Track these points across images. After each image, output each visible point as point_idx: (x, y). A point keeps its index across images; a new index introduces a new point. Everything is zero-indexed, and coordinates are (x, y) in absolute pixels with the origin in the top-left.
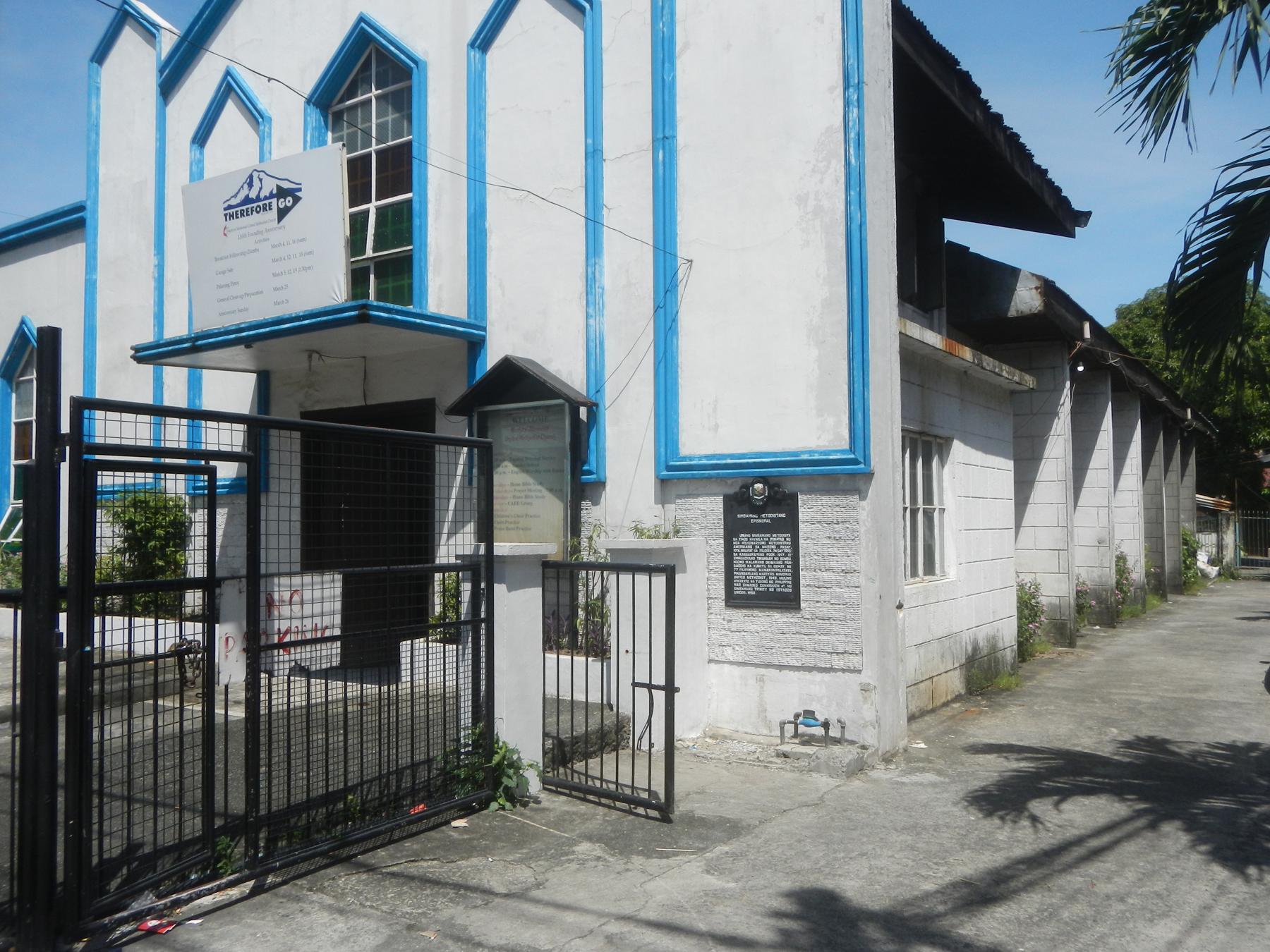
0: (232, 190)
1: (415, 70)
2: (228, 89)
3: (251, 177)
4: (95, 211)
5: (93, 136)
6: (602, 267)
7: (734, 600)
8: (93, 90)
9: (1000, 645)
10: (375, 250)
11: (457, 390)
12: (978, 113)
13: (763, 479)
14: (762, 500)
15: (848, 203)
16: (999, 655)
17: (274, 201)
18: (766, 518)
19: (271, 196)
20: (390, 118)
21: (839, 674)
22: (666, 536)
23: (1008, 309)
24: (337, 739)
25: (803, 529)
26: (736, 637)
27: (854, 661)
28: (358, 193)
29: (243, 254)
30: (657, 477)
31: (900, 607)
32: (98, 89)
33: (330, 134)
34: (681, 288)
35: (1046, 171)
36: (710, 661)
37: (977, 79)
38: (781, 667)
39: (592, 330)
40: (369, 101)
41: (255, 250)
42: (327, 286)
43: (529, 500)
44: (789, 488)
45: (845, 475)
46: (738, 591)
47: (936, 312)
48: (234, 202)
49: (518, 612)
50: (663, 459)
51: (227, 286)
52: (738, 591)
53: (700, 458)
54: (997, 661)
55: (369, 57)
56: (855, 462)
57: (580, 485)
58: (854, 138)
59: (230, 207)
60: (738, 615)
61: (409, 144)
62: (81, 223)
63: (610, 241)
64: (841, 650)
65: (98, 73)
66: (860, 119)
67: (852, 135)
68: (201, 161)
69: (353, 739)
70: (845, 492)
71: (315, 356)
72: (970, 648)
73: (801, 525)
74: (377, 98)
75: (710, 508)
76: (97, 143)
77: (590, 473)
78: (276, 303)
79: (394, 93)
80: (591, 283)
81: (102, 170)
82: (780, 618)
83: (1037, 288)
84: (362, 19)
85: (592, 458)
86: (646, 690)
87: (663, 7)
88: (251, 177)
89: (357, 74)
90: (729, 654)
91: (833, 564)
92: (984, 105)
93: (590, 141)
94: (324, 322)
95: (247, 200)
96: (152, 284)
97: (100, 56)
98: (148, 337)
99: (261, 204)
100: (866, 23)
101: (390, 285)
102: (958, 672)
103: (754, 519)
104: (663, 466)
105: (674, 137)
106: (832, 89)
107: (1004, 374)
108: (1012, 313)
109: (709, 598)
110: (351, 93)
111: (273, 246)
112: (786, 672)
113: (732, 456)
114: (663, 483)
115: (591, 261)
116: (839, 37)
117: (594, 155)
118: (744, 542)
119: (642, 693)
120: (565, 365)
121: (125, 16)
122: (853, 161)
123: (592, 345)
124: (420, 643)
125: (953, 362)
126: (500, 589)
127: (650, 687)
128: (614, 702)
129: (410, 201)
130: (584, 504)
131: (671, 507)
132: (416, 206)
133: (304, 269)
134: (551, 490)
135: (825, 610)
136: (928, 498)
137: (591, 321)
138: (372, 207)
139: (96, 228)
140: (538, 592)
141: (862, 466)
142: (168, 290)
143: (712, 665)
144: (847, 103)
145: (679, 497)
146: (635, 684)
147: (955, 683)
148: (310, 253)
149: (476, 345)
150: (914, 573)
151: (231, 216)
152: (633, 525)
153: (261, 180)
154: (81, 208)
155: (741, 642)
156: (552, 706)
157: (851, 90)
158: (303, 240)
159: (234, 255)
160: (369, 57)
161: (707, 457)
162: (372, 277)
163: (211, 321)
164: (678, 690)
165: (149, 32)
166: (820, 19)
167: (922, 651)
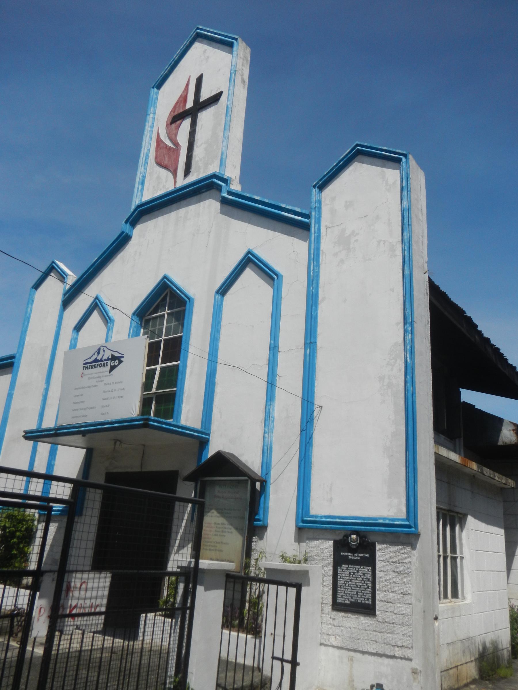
0: (88, 355)
1: (188, 303)
2: (96, 305)
3: (99, 349)
4: (20, 359)
5: (26, 323)
6: (274, 406)
7: (337, 606)
8: (31, 301)
9: (500, 647)
10: (157, 389)
11: (191, 467)
12: (477, 337)
13: (356, 532)
14: (356, 545)
15: (406, 382)
16: (499, 653)
17: (109, 362)
18: (357, 556)
19: (108, 359)
20: (173, 324)
21: (399, 660)
22: (300, 562)
23: (498, 441)
24: (93, 676)
25: (379, 565)
26: (337, 630)
27: (408, 653)
28: (152, 360)
29: (89, 387)
30: (297, 526)
31: (436, 619)
32: (33, 301)
33: (142, 330)
34: (315, 421)
35: (515, 368)
36: (321, 644)
37: (475, 321)
38: (363, 653)
39: (266, 440)
40: (164, 315)
41: (96, 386)
42: (130, 407)
43: (224, 534)
44: (371, 539)
45: (403, 534)
46: (340, 600)
47: (457, 440)
49: (209, 603)
50: (300, 516)
51: (79, 403)
52: (340, 600)
53: (321, 517)
54: (498, 658)
55: (166, 296)
56: (409, 527)
57: (254, 527)
58: (409, 349)
59: (87, 363)
60: (340, 616)
61: (181, 337)
62: (11, 365)
63: (279, 394)
64: (400, 644)
65: (34, 294)
66: (412, 339)
67: (408, 347)
69: (103, 677)
70: (403, 544)
71: (118, 443)
72: (481, 648)
73: (378, 562)
74: (168, 314)
75: (325, 548)
76: (27, 326)
77: (259, 520)
78: (102, 414)
79: (177, 312)
80: (268, 414)
81: (27, 339)
82: (364, 621)
83: (513, 430)
84: (165, 277)
85: (261, 512)
86: (279, 663)
87: (313, 280)
88: (99, 349)
89: (159, 302)
90: (333, 641)
91: (396, 588)
92: (480, 333)
93: (272, 342)
94: (125, 426)
95: (96, 361)
96: (41, 398)
97: (37, 286)
99: (102, 363)
100: (415, 293)
101: (163, 408)
102: (473, 664)
103: (351, 556)
104: (300, 520)
105: (316, 343)
106: (398, 324)
107: (496, 478)
108: (500, 443)
109: (322, 603)
110: (155, 311)
111: (106, 384)
112: (366, 656)
113: (339, 517)
114: (300, 530)
115: (269, 403)
116: (401, 298)
117: (274, 349)
118: (344, 570)
119: (277, 664)
120: (251, 459)
121: (52, 269)
122: (409, 360)
123: (266, 448)
124: (151, 616)
125: (466, 470)
126: (200, 589)
127: (282, 660)
128: (261, 666)
129: (178, 366)
130: (255, 539)
131: (303, 545)
132: (181, 368)
133: (119, 397)
134: (236, 529)
135: (390, 617)
136: (454, 549)
137: (266, 435)
138: (158, 367)
139: (18, 367)
140: (221, 593)
141: (413, 529)
142: (49, 401)
143: (322, 647)
144: (405, 331)
145: (309, 539)
146: (273, 658)
147: (471, 671)
148: (124, 389)
149: (203, 443)
150: (446, 597)
151: (87, 368)
152: (281, 554)
153: (104, 351)
154: (13, 357)
155: (340, 633)
156: (224, 665)
157: (408, 325)
158: (121, 382)
159: (84, 388)
160: (166, 295)
161: (326, 517)
162: (154, 403)
163: (67, 420)
164: (298, 664)
165: (62, 277)
166: (392, 290)
167: (451, 648)
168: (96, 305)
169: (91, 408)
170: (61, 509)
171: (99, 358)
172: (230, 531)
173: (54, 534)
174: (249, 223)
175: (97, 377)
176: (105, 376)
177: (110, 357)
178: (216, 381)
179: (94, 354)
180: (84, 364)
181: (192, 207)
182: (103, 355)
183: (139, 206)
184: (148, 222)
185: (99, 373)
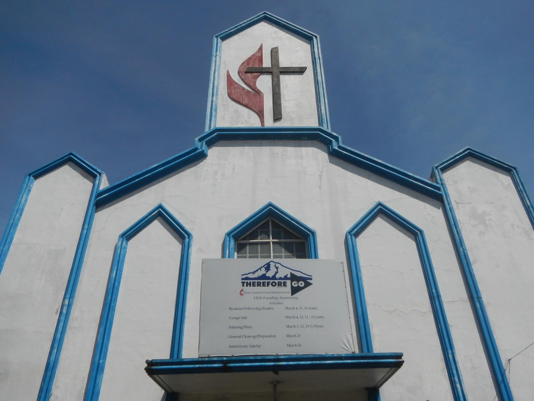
19: (286, 278)
32: (30, 191)
33: (236, 253)
41: (270, 308)
48: (251, 276)
59: (247, 278)
65: (32, 183)
68: (125, 248)
74: (273, 243)
78: (289, 345)
89: (258, 228)
95: (264, 277)
98: (165, 355)
99: (277, 281)
111: (287, 308)
142: (72, 323)
153: (277, 268)
158: (315, 308)
159: (249, 309)
168: (161, 214)
169: (267, 336)
171: (270, 274)
174: (369, 179)
175: (272, 298)
177: (289, 276)
179: (260, 269)
180: (242, 279)
181: (290, 149)
182: (276, 273)
183: (217, 130)
184: (230, 148)
185: (273, 293)
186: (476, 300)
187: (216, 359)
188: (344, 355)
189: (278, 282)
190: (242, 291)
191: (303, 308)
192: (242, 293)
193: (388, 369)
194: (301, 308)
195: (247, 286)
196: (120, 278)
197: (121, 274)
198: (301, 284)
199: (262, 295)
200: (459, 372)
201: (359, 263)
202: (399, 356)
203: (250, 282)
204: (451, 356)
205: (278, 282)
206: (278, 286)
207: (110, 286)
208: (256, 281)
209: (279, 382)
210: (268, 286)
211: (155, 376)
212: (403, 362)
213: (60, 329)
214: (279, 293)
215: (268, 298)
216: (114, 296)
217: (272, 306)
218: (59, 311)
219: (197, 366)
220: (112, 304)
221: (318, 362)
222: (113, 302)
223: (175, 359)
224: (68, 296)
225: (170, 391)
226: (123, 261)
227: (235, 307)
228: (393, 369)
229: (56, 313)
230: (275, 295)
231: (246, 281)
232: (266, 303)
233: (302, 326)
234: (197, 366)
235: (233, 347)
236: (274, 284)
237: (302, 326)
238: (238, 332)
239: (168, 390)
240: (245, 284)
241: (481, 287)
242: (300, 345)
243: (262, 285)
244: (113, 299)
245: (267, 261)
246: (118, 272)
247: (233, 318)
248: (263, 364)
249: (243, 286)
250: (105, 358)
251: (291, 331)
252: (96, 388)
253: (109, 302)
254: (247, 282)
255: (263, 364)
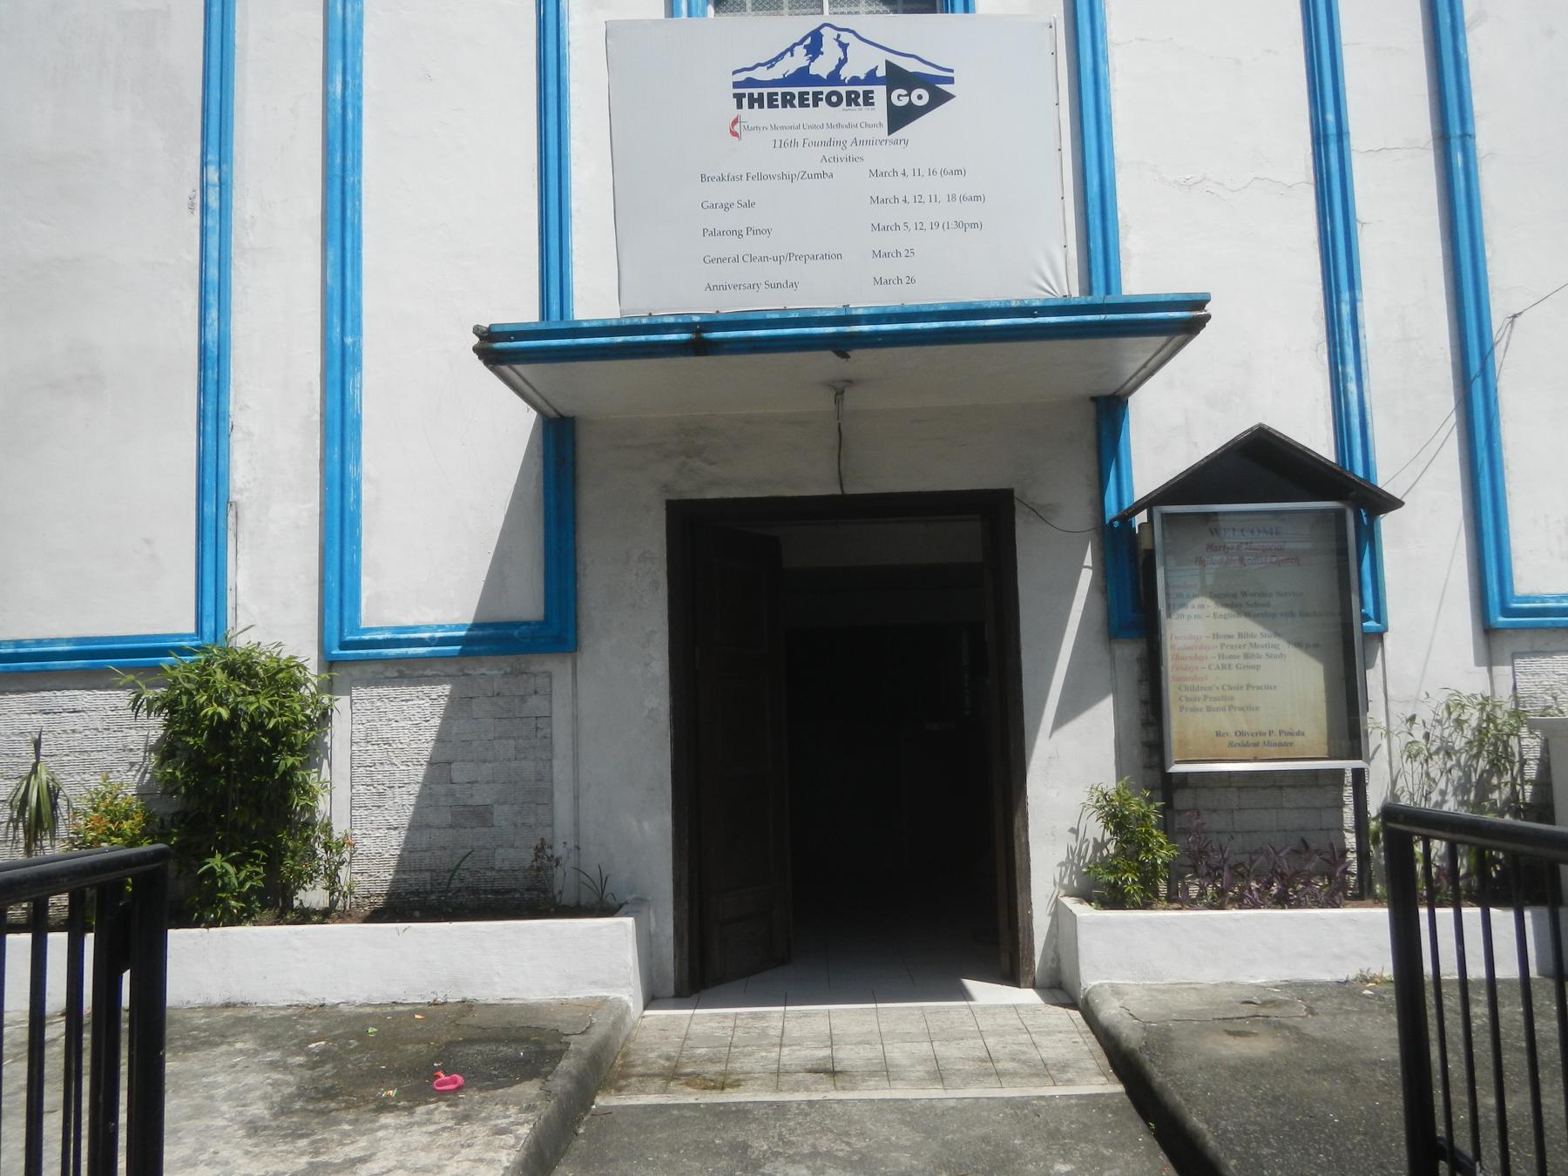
19: (871, 78)
43: (1252, 662)
48: (761, 74)
59: (750, 83)
78: (879, 281)
95: (802, 77)
99: (843, 90)
111: (875, 174)
114: (1488, 632)
131: (1503, 672)
134: (1298, 645)
153: (844, 47)
158: (958, 172)
159: (760, 177)
170: (463, 633)
171: (822, 67)
172: (1272, 651)
173: (437, 721)
175: (830, 143)
176: (868, 142)
177: (881, 72)
178: (1120, 216)
179: (791, 50)
180: (736, 85)
182: (842, 62)
186: (1456, 144)
187: (672, 320)
188: (1038, 303)
189: (849, 93)
190: (735, 122)
191: (924, 172)
192: (737, 128)
193: (1163, 339)
194: (917, 173)
195: (751, 106)
196: (360, 98)
197: (360, 86)
198: (920, 97)
199: (799, 135)
200: (1363, 351)
201: (1104, 32)
202: (1199, 303)
203: (761, 95)
204: (1345, 309)
205: (849, 93)
206: (849, 104)
207: (331, 123)
208: (780, 90)
209: (850, 382)
210: (815, 105)
211: (505, 368)
212: (1208, 317)
213: (213, 253)
214: (849, 126)
215: (815, 144)
216: (349, 154)
217: (827, 168)
218: (198, 201)
219: (620, 339)
220: (349, 180)
221: (963, 323)
222: (349, 173)
223: (555, 322)
224: (213, 156)
225: (553, 414)
226: (359, 44)
227: (718, 174)
228: (1178, 338)
229: (191, 208)
230: (837, 134)
231: (747, 91)
232: (810, 159)
233: (919, 227)
234: (620, 339)
235: (718, 287)
236: (834, 99)
237: (919, 227)
238: (729, 246)
239: (546, 408)
240: (745, 101)
241: (1481, 101)
242: (911, 280)
243: (796, 102)
244: (349, 162)
245: (809, 23)
246: (349, 78)
247: (714, 206)
248: (807, 330)
249: (740, 106)
250: (358, 330)
251: (887, 241)
252: (349, 411)
253: (338, 172)
254: (751, 95)
255: (807, 330)
